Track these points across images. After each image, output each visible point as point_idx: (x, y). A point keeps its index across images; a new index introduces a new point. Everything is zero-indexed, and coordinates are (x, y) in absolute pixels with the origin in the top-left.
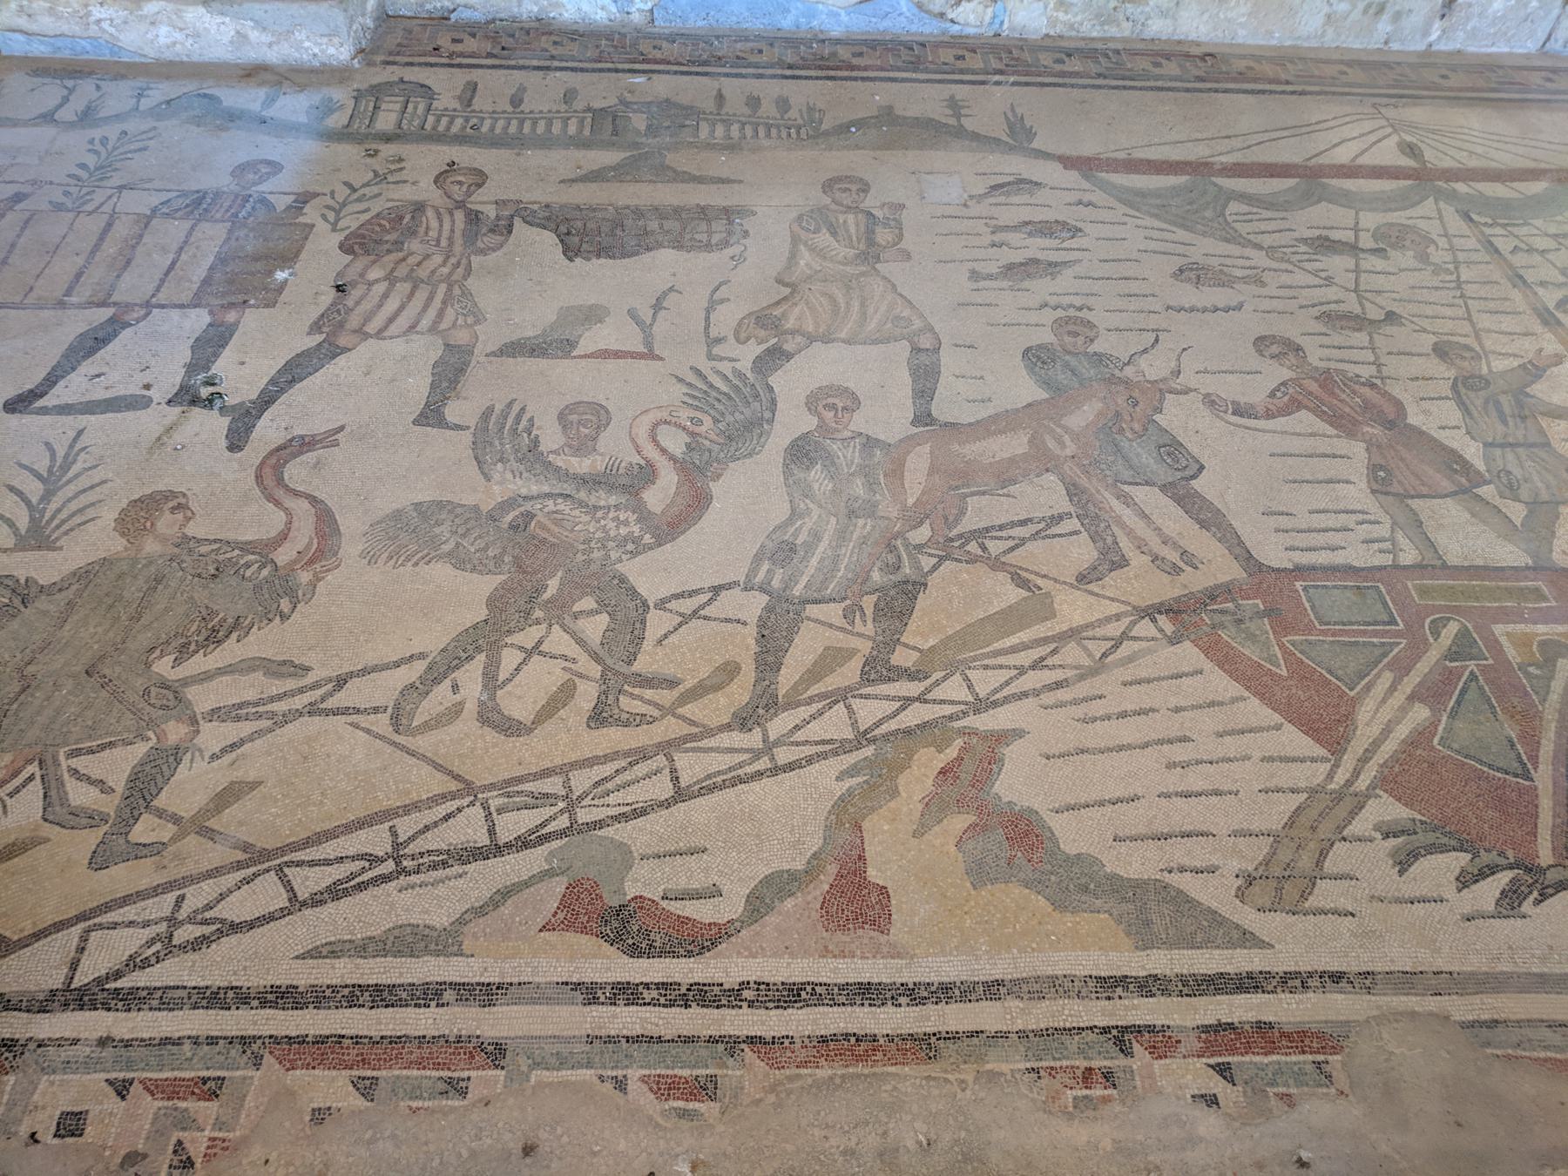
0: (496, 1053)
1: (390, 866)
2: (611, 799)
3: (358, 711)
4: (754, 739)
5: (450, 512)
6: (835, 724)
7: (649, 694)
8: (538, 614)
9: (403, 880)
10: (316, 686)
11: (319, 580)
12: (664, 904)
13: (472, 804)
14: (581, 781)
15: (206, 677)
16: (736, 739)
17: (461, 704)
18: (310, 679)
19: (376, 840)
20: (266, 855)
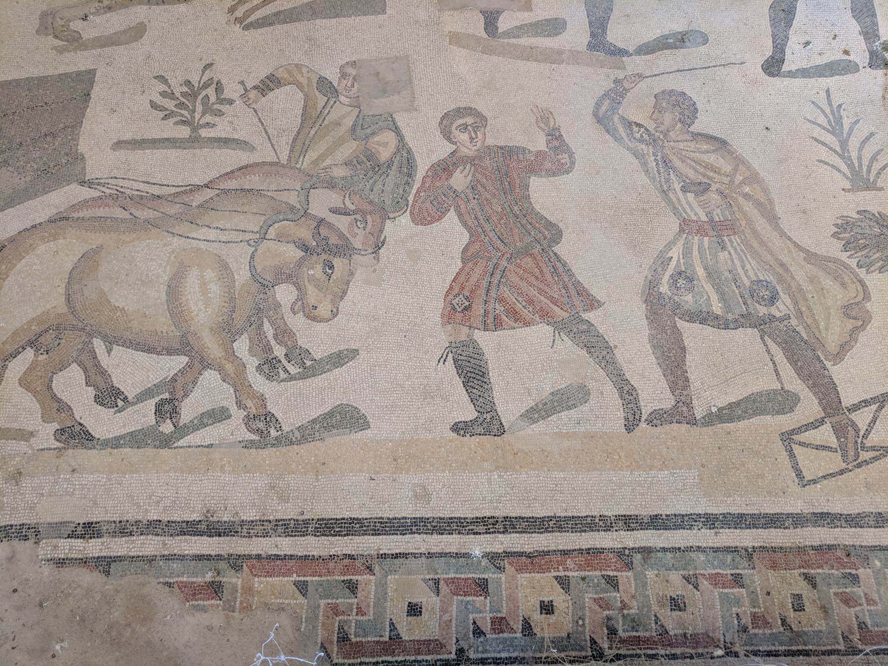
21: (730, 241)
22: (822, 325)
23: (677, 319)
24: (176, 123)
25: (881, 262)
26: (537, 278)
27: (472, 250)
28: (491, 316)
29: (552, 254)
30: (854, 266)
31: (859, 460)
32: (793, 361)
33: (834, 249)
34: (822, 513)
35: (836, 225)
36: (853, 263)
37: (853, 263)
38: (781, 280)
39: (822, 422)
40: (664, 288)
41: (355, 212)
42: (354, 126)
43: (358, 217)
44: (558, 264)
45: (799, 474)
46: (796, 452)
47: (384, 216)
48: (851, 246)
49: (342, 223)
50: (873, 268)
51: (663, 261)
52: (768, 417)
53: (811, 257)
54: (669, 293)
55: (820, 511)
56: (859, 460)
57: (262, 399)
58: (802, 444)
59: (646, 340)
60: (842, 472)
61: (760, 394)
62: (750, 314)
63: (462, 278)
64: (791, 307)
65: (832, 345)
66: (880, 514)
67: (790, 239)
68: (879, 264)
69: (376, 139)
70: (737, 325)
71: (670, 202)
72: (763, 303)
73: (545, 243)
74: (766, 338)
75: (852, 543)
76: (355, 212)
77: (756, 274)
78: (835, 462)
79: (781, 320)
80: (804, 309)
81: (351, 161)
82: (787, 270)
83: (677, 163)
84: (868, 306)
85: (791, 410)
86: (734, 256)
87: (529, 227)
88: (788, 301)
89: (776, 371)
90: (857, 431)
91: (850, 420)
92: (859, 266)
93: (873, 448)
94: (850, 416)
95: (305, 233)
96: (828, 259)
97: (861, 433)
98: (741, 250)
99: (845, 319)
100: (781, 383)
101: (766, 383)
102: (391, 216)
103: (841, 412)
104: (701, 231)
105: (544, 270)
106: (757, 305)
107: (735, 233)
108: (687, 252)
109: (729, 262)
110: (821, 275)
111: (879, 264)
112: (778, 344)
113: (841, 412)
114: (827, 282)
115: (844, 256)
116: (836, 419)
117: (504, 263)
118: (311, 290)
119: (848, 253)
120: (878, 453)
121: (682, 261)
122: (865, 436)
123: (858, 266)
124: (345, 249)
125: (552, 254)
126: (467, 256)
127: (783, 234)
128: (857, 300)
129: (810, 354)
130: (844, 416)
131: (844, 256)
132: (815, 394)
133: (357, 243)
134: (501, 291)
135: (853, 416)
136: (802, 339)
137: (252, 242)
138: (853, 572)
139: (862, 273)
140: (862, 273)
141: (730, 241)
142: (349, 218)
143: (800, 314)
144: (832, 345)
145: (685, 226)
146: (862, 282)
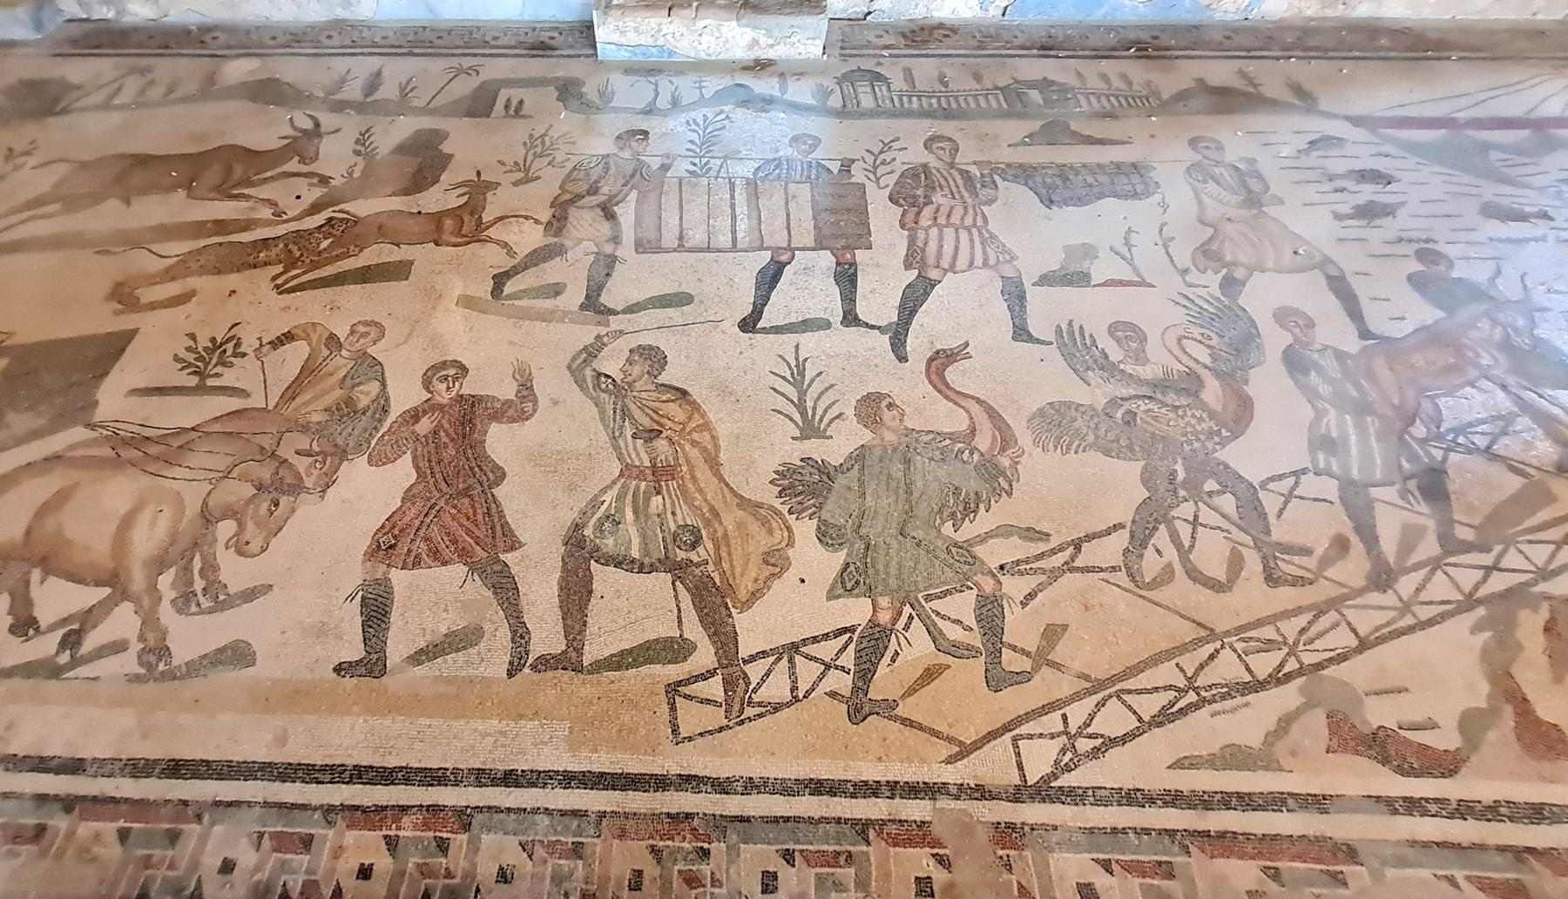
0: (1351, 853)
1: (1192, 697)
2: (1318, 644)
3: (1102, 570)
4: (1389, 599)
5: (1077, 410)
6: (1440, 588)
7: (1296, 559)
8: (1182, 493)
9: (1208, 709)
10: (1061, 549)
11: (1017, 463)
12: (1400, 731)
13: (1223, 647)
14: (1290, 628)
15: (983, 539)
16: (1375, 598)
17: (1170, 565)
18: (1054, 542)
19: (1166, 673)
20: (1098, 686)
21: (667, 485)
22: (738, 570)
23: (592, 561)
24: (190, 374)
25: (814, 509)
26: (468, 519)
27: (415, 491)
28: (413, 555)
29: (489, 495)
30: (785, 512)
31: (742, 717)
32: (699, 608)
33: (769, 496)
34: (689, 775)
35: (776, 472)
36: (785, 509)
37: (785, 509)
38: (708, 523)
39: (712, 673)
40: (588, 532)
41: (317, 454)
42: (345, 376)
43: (319, 458)
44: (493, 505)
45: (675, 731)
46: (678, 705)
47: (342, 455)
48: (787, 492)
49: (302, 464)
50: (803, 515)
51: (595, 503)
52: (658, 666)
53: (743, 502)
54: (592, 536)
55: (687, 773)
56: (742, 717)
57: (164, 633)
58: (686, 697)
59: (555, 583)
60: (721, 730)
61: (657, 641)
62: (667, 558)
63: (396, 518)
64: (712, 553)
65: (743, 595)
66: (751, 779)
67: (727, 485)
68: (810, 511)
69: (361, 388)
70: (653, 569)
71: (617, 448)
72: (684, 548)
73: (486, 484)
74: (678, 583)
75: (711, 812)
76: (317, 454)
77: (684, 519)
78: (717, 717)
79: (698, 565)
80: (724, 555)
81: (332, 407)
82: (716, 515)
83: (633, 407)
84: (790, 552)
85: (685, 659)
86: (668, 501)
87: (476, 469)
88: (710, 545)
89: (679, 618)
90: (748, 684)
91: (744, 673)
92: (791, 513)
93: (760, 704)
94: (744, 668)
95: (265, 473)
96: (760, 505)
97: (751, 688)
98: (676, 495)
99: (764, 566)
100: (681, 630)
101: (668, 630)
102: (350, 457)
103: (736, 662)
104: (641, 476)
105: (478, 511)
106: (677, 550)
107: (673, 479)
108: (620, 498)
109: (661, 507)
110: (751, 519)
111: (810, 511)
112: (688, 590)
113: (736, 662)
114: (754, 527)
115: (777, 503)
116: (730, 670)
117: (442, 503)
118: (250, 526)
119: (782, 500)
120: (763, 710)
121: (614, 505)
122: (755, 691)
123: (789, 511)
124: (297, 488)
125: (489, 495)
126: (409, 496)
127: (722, 479)
128: (780, 546)
129: (719, 600)
130: (738, 668)
131: (777, 503)
132: (714, 643)
133: (309, 483)
134: (430, 530)
135: (747, 668)
136: (715, 583)
137: (213, 481)
138: (706, 846)
139: (791, 519)
140: (791, 519)
141: (667, 485)
142: (311, 459)
143: (718, 562)
144: (743, 595)
145: (627, 471)
146: (789, 528)
